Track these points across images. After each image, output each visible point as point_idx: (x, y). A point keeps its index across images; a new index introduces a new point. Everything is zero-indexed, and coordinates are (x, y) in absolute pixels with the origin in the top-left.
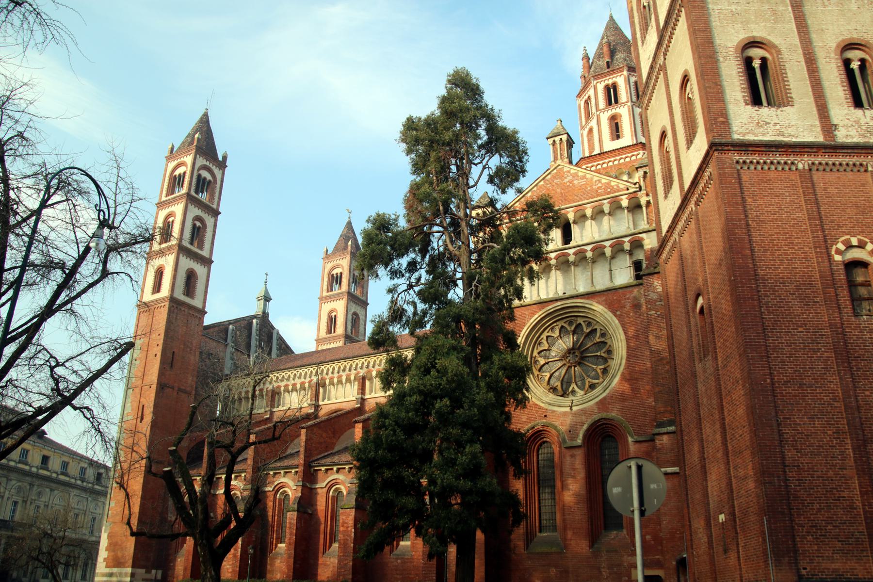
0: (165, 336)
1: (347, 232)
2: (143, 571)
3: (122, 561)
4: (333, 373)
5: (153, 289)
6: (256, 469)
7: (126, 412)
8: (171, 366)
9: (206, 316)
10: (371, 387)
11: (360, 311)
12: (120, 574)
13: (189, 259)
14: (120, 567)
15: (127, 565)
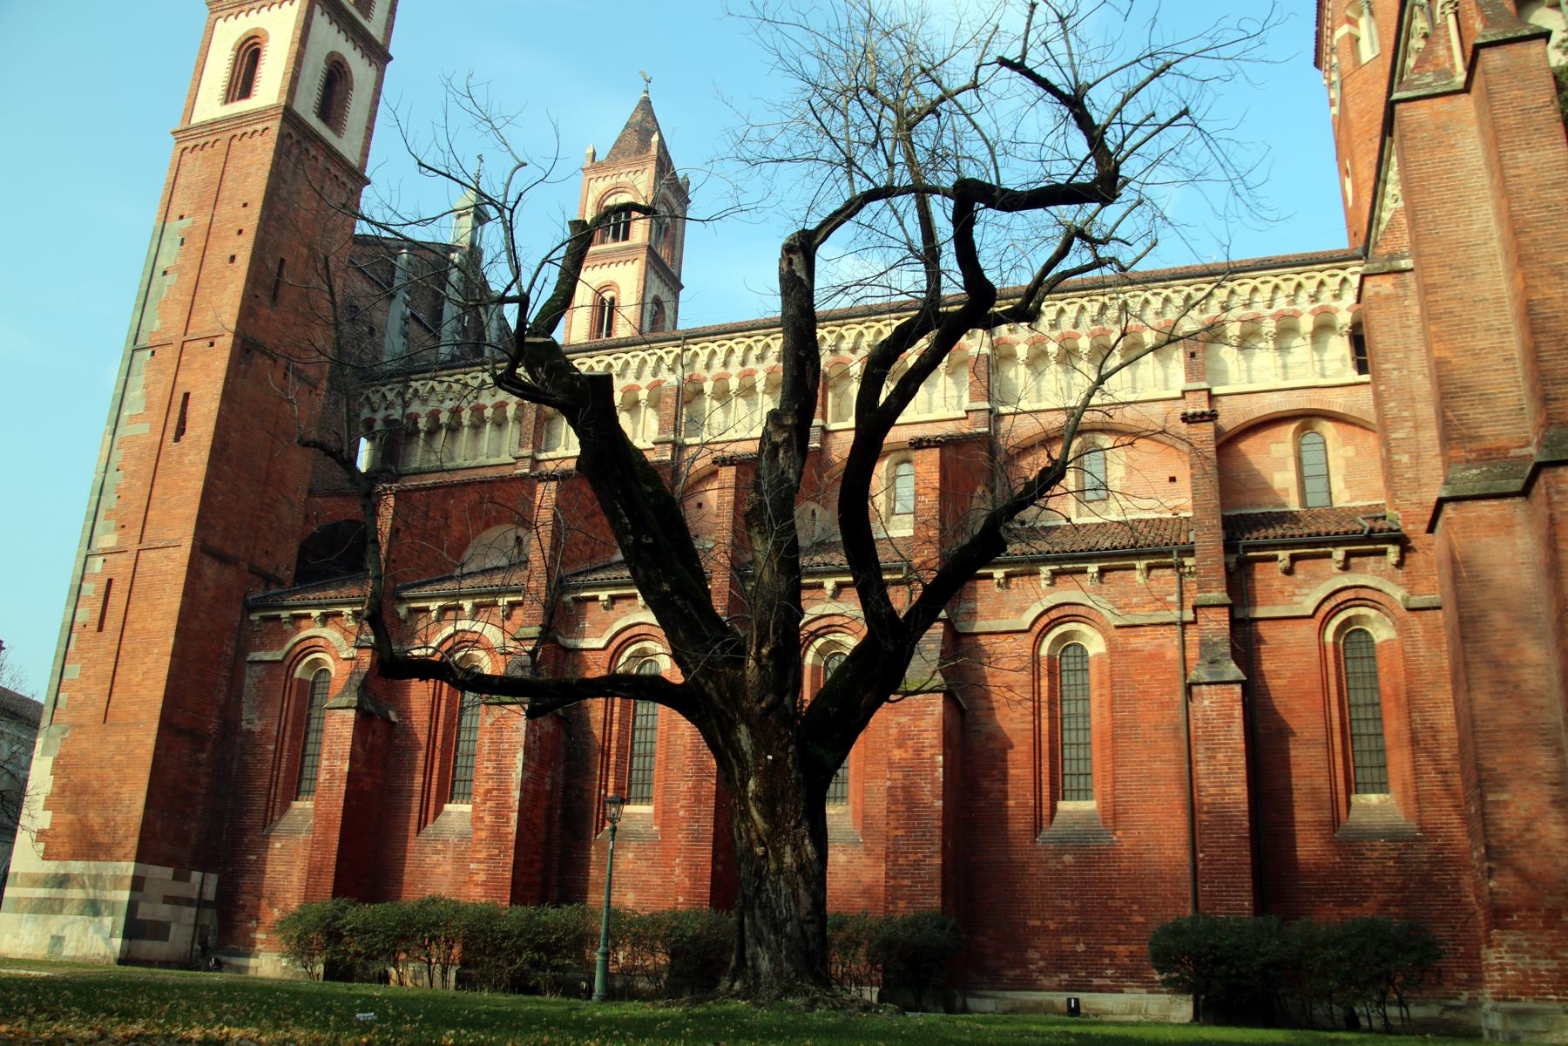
0: (264, 208)
1: (643, 120)
2: (169, 872)
3: (106, 839)
4: (725, 364)
5: (228, 91)
6: (558, 586)
7: (125, 413)
8: (274, 298)
9: (366, 190)
10: (838, 406)
11: (665, 295)
12: (97, 880)
13: (335, 28)
14: (96, 858)
15: (120, 852)
